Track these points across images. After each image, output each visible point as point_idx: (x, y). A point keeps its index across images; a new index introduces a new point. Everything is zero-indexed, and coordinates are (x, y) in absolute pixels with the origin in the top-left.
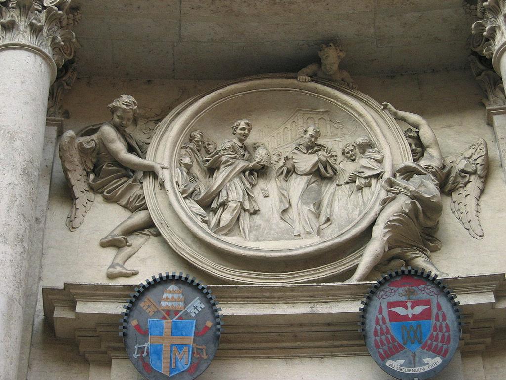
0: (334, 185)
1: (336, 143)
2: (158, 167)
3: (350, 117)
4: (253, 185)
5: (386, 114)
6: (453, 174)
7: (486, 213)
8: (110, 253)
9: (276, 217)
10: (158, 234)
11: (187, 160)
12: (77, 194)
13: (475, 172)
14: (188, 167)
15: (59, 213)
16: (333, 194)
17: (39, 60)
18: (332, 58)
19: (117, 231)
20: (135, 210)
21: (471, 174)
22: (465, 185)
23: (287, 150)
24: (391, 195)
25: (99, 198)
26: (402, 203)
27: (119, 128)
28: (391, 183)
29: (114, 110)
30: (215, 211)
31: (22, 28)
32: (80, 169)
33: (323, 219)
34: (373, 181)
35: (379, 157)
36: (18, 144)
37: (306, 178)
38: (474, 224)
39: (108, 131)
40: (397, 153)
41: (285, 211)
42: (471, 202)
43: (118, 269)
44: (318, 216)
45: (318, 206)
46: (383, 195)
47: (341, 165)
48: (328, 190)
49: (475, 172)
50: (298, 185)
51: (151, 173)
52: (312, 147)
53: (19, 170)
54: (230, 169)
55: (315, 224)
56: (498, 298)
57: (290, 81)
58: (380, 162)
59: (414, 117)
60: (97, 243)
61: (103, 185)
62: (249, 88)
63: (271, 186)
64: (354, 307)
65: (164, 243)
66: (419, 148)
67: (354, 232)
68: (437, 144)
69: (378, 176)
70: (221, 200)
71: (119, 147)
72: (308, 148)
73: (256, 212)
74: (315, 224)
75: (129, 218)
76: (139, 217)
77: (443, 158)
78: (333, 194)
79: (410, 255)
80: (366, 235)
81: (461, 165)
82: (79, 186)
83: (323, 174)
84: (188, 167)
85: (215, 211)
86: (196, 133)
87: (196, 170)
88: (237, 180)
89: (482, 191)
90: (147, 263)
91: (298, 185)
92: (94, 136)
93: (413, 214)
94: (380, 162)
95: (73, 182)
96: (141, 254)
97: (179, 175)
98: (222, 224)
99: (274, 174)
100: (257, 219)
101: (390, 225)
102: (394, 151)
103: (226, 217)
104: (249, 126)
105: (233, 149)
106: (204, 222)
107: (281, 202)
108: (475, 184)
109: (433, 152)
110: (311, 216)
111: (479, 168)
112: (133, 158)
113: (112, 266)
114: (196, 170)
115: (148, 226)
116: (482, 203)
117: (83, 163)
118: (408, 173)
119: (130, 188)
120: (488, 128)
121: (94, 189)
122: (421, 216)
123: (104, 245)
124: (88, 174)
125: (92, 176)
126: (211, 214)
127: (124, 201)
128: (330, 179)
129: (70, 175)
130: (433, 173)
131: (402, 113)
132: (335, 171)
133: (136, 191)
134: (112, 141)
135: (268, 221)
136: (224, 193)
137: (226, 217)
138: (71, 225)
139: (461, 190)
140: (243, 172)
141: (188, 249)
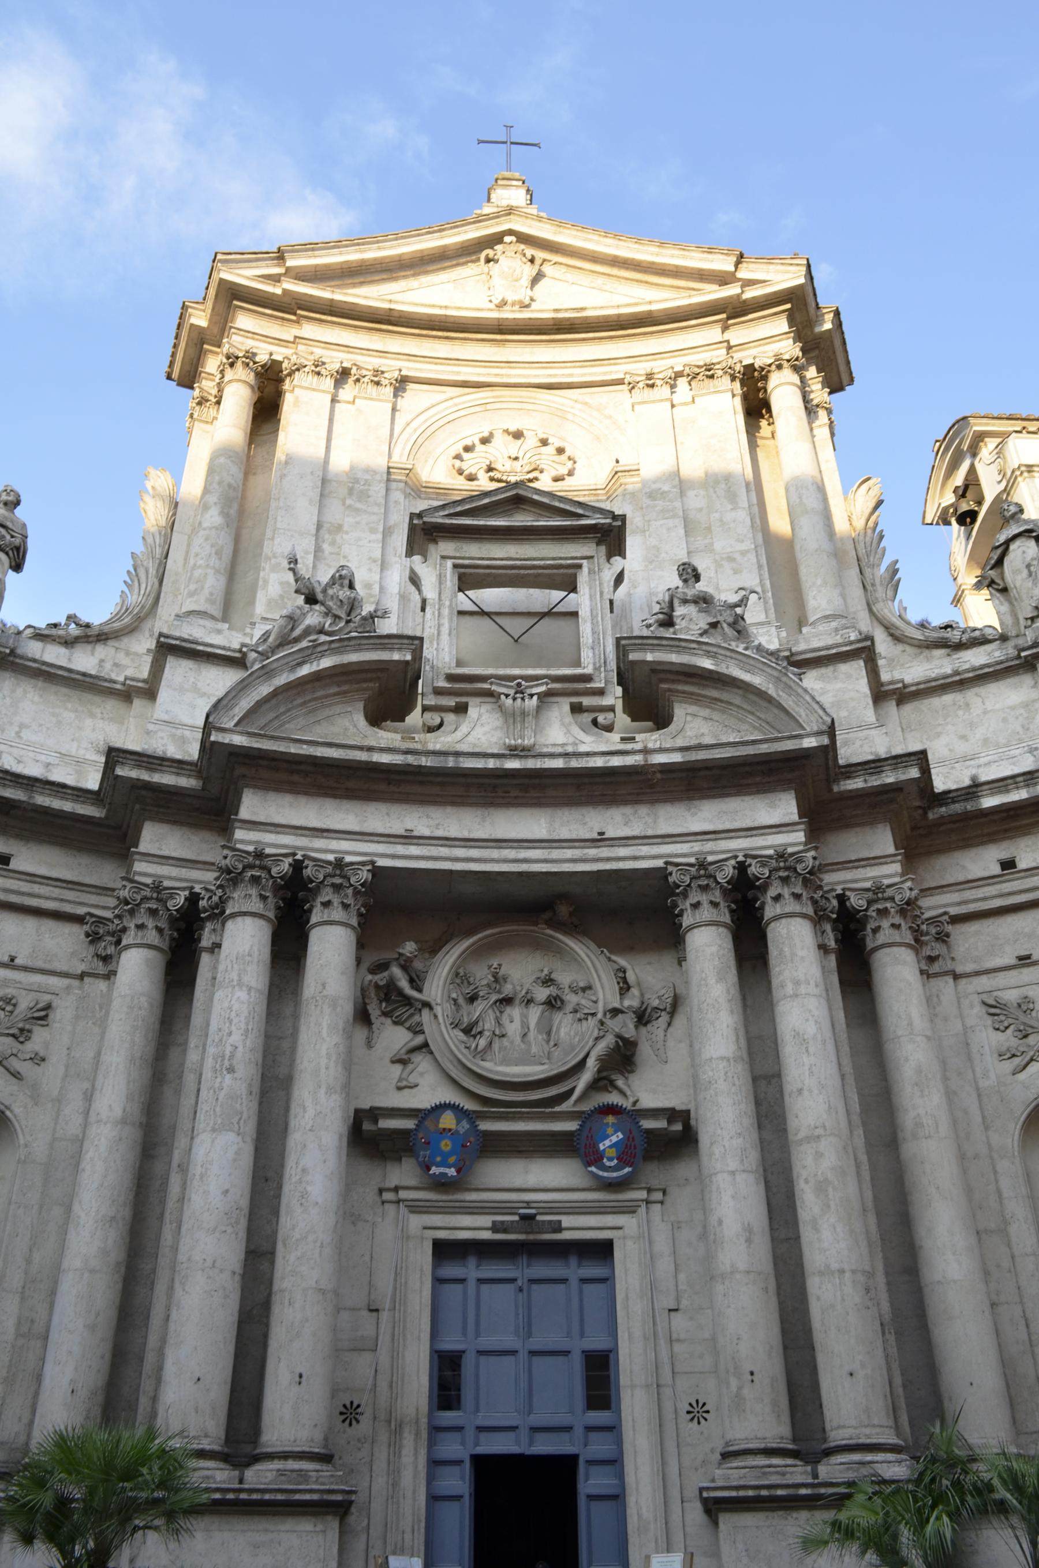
0: (561, 1014)
1: (564, 978)
2: (433, 1003)
3: (576, 960)
4: (501, 1012)
5: (602, 958)
6: (649, 1010)
7: (671, 1043)
8: (398, 1068)
9: (518, 1039)
10: (432, 1053)
11: (454, 995)
12: (373, 1019)
13: (665, 1009)
14: (455, 1000)
15: (360, 1034)
16: (560, 1022)
17: (349, 930)
18: (563, 910)
19: (403, 1051)
20: (416, 1033)
21: (662, 1010)
22: (657, 1018)
23: (528, 982)
24: (602, 1034)
25: (388, 1021)
26: (609, 1040)
27: (405, 968)
28: (602, 1023)
29: (400, 954)
30: (474, 1036)
31: (335, 904)
32: (375, 1001)
33: (552, 1043)
34: (590, 1018)
35: (594, 999)
36: (339, 1009)
37: (541, 1007)
38: (662, 1051)
39: (396, 971)
40: (609, 996)
41: (525, 1035)
42: (660, 1032)
43: (404, 1083)
44: (548, 1041)
45: (549, 1033)
46: (596, 1034)
47: (568, 997)
48: (558, 1017)
49: (665, 1009)
50: (534, 1014)
51: (427, 1005)
52: (547, 982)
53: (341, 1032)
54: (486, 1002)
55: (546, 1048)
56: (669, 1122)
57: (532, 928)
58: (595, 1002)
59: (622, 962)
60: (387, 1061)
61: (392, 1011)
62: (501, 933)
63: (515, 1012)
64: (571, 1126)
65: (436, 1060)
66: (625, 987)
67: (573, 1063)
68: (639, 984)
69: (593, 1014)
70: (479, 1030)
71: (404, 984)
72: (543, 983)
73: (503, 1036)
74: (546, 1048)
75: (411, 1040)
76: (419, 1040)
77: (642, 995)
78: (560, 1022)
79: (613, 1077)
80: (581, 1065)
81: (656, 1003)
82: (374, 1011)
83: (553, 1004)
84: (455, 1000)
85: (474, 1036)
86: (461, 971)
87: (461, 1001)
88: (490, 1011)
89: (669, 1024)
90: (428, 1090)
91: (534, 1014)
92: (386, 974)
94: (595, 1002)
95: (370, 1011)
96: (420, 1069)
97: (449, 1007)
98: (480, 1048)
99: (517, 1002)
100: (505, 1039)
101: (599, 1059)
102: (607, 994)
103: (482, 1042)
104: (500, 965)
105: (488, 985)
106: (466, 1048)
107: (522, 1027)
108: (664, 1018)
109: (635, 991)
110: (544, 1043)
111: (668, 1006)
112: (414, 994)
113: (400, 1080)
114: (461, 1001)
115: (426, 1045)
116: (668, 1034)
117: (377, 995)
118: (615, 1012)
119: (412, 1015)
120: (678, 967)
121: (385, 1014)
122: (623, 1049)
123: (393, 1062)
124: (381, 1002)
125: (384, 1005)
126: (472, 1039)
127: (407, 1025)
128: (559, 1008)
129: (368, 1007)
130: (634, 1012)
131: (614, 958)
132: (562, 1001)
133: (416, 1018)
134: (399, 980)
135: (512, 1043)
136: (480, 1023)
137: (482, 1042)
138: (369, 1044)
139: (654, 1023)
140: (495, 1002)
141: (454, 1070)
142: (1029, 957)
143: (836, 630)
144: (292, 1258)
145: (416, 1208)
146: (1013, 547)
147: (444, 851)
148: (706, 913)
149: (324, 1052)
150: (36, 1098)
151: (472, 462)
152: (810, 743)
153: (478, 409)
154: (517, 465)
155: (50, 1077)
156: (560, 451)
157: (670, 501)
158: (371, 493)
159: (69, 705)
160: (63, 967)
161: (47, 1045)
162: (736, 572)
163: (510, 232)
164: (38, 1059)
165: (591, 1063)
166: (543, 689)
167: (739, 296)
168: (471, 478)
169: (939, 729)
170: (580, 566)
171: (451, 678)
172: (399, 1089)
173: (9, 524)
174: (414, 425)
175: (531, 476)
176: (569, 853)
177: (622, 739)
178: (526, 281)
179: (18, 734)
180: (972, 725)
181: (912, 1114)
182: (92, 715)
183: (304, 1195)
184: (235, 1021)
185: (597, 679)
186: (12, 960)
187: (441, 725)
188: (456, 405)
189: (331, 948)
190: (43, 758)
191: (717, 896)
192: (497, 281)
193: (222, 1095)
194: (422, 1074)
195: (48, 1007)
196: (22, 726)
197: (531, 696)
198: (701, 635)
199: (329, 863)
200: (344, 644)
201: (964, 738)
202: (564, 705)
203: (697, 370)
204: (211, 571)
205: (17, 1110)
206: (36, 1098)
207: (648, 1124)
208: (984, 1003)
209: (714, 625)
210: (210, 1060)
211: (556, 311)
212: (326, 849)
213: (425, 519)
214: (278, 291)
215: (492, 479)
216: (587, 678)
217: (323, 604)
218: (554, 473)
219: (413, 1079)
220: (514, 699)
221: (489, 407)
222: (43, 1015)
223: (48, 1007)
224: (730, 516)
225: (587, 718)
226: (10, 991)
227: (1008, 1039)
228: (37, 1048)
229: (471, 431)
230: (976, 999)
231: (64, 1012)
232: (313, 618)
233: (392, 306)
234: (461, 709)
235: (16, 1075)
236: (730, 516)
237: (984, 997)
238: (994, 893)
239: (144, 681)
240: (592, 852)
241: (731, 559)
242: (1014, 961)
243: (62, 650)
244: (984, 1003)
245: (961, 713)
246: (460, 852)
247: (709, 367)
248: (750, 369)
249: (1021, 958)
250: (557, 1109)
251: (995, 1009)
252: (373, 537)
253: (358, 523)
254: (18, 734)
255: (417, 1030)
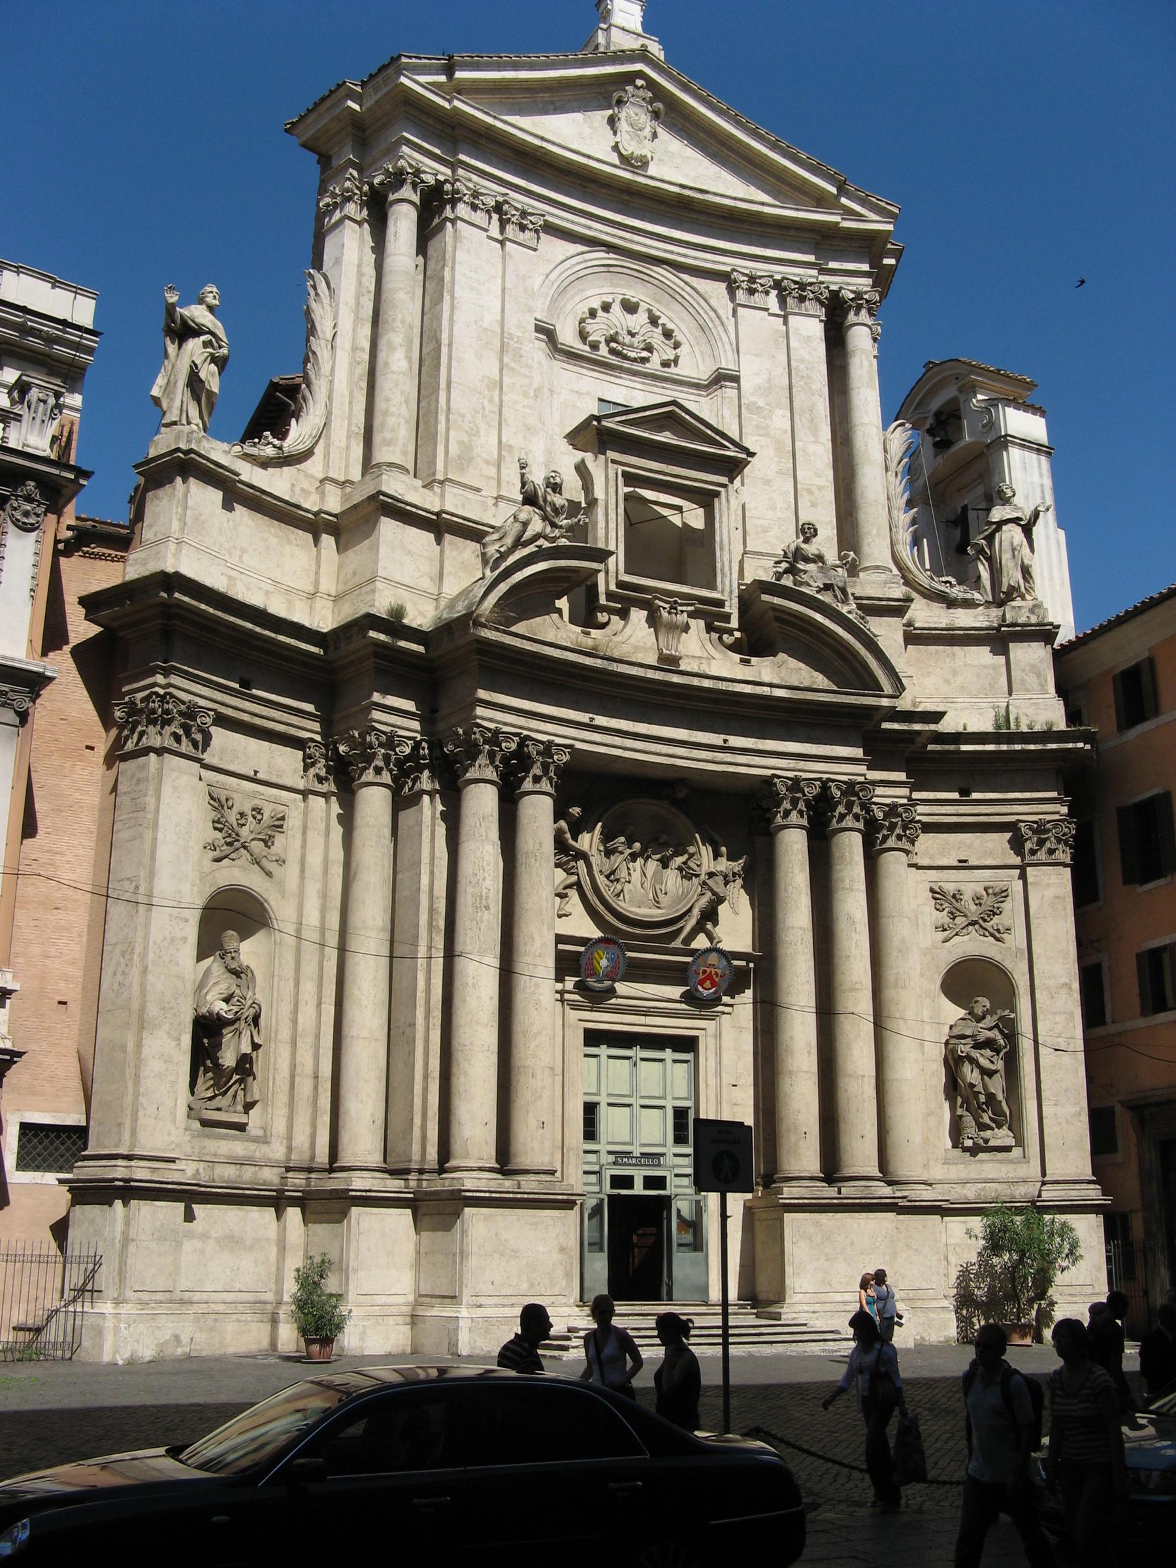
8: (558, 899)
69: (697, 876)
71: (568, 835)
75: (565, 880)
76: (574, 878)
93: (711, 901)
103: (619, 887)
112: (573, 843)
118: (711, 875)
137: (619, 887)
142: (965, 861)
143: (885, 582)
144: (533, 1045)
145: (575, 1007)
146: (1004, 528)
147: (617, 741)
148: (794, 817)
149: (544, 898)
150: (283, 894)
151: (596, 327)
152: (885, 702)
153: (603, 269)
154: (635, 340)
155: (290, 873)
156: (668, 334)
157: (764, 417)
158: (523, 352)
159: (273, 530)
160: (288, 782)
161: (285, 849)
162: (814, 505)
163: (640, 74)
164: (281, 862)
165: (696, 912)
166: (691, 608)
167: (838, 223)
168: (595, 346)
169: (931, 669)
170: (717, 494)
171: (621, 585)
172: (560, 916)
173: (217, 332)
174: (552, 277)
175: (645, 354)
176: (704, 754)
177: (742, 660)
178: (647, 132)
179: (241, 557)
180: (954, 673)
181: (895, 971)
182: (289, 542)
183: (538, 1003)
184: (487, 868)
185: (727, 604)
186: (256, 772)
187: (607, 624)
188: (586, 261)
189: (538, 813)
190: (262, 585)
191: (801, 805)
192: (623, 126)
193: (483, 926)
194: (574, 905)
195: (283, 818)
196: (243, 551)
197: (682, 612)
198: (818, 592)
199: (542, 742)
200: (557, 553)
201: (947, 681)
202: (702, 623)
203: (793, 286)
204: (402, 421)
205: (272, 903)
206: (283, 894)
207: (735, 963)
208: (932, 890)
209: (828, 587)
210: (470, 896)
211: (682, 186)
212: (543, 732)
213: (604, 423)
214: (446, 105)
215: (613, 352)
216: (720, 603)
217: (540, 508)
218: (666, 357)
219: (568, 909)
220: (670, 613)
221: (611, 269)
222: (278, 825)
223: (283, 818)
224: (811, 448)
225: (715, 636)
226: (257, 802)
227: (943, 918)
228: (279, 851)
229: (595, 293)
230: (928, 886)
231: (293, 822)
232: (537, 525)
233: (545, 145)
234: (624, 614)
235: (269, 874)
236: (811, 448)
237: (932, 885)
238: (953, 812)
239: (335, 516)
240: (720, 756)
241: (810, 492)
242: (956, 863)
243: (258, 471)
244: (932, 890)
245: (948, 660)
246: (629, 743)
247: (802, 286)
248: (835, 295)
249: (960, 861)
250: (673, 945)
251: (937, 894)
252: (526, 402)
253: (513, 384)
254: (241, 557)
255: (569, 872)
